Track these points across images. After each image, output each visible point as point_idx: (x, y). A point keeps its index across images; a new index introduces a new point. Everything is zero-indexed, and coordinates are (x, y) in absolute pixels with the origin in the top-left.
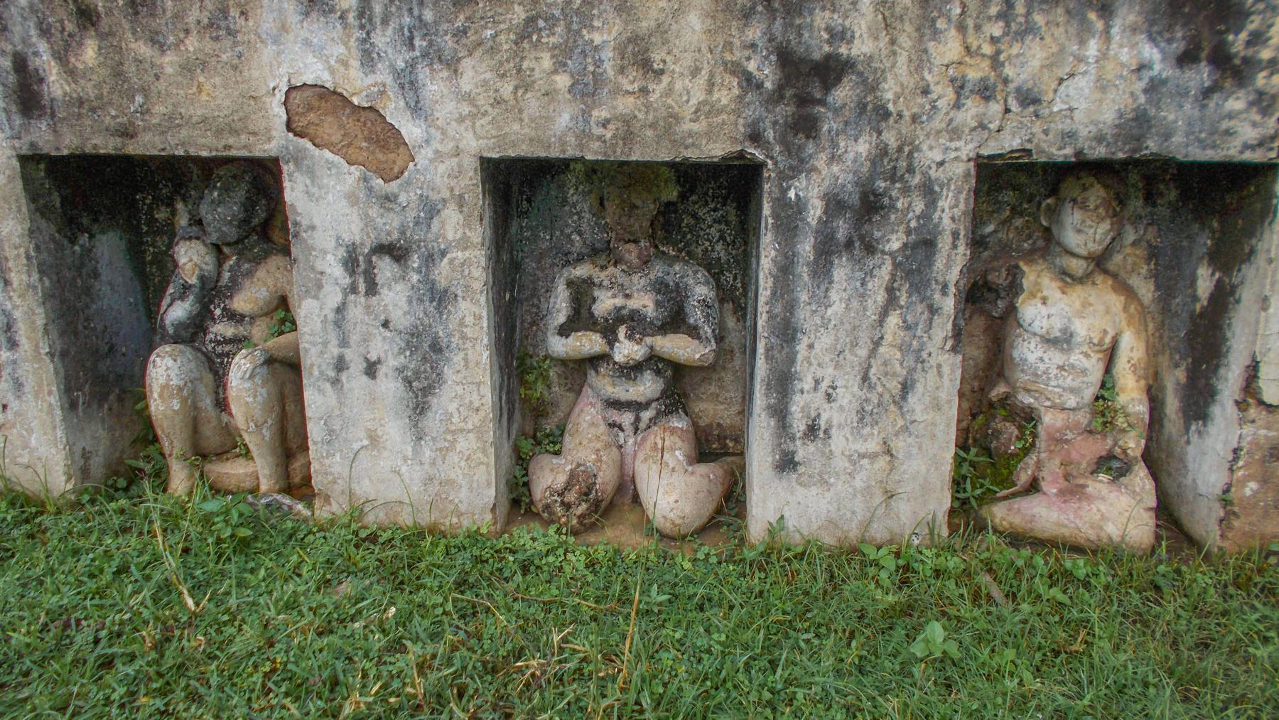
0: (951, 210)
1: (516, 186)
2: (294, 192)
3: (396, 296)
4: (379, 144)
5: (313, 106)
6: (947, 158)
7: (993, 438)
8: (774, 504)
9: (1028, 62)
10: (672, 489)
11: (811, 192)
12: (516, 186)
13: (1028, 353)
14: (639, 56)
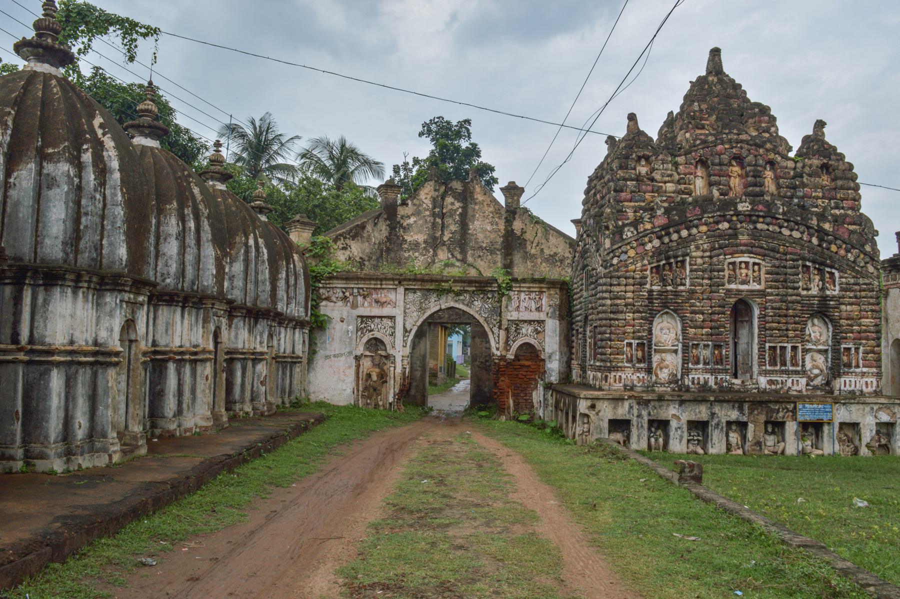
0: (724, 425)
1: (690, 423)
2: (671, 423)
3: (679, 432)
4: (679, 419)
5: (674, 415)
6: (724, 421)
7: (729, 447)
8: (712, 451)
9: (729, 414)
10: (701, 451)
11: (713, 423)
12: (690, 423)
13: (730, 439)
14: (700, 412)
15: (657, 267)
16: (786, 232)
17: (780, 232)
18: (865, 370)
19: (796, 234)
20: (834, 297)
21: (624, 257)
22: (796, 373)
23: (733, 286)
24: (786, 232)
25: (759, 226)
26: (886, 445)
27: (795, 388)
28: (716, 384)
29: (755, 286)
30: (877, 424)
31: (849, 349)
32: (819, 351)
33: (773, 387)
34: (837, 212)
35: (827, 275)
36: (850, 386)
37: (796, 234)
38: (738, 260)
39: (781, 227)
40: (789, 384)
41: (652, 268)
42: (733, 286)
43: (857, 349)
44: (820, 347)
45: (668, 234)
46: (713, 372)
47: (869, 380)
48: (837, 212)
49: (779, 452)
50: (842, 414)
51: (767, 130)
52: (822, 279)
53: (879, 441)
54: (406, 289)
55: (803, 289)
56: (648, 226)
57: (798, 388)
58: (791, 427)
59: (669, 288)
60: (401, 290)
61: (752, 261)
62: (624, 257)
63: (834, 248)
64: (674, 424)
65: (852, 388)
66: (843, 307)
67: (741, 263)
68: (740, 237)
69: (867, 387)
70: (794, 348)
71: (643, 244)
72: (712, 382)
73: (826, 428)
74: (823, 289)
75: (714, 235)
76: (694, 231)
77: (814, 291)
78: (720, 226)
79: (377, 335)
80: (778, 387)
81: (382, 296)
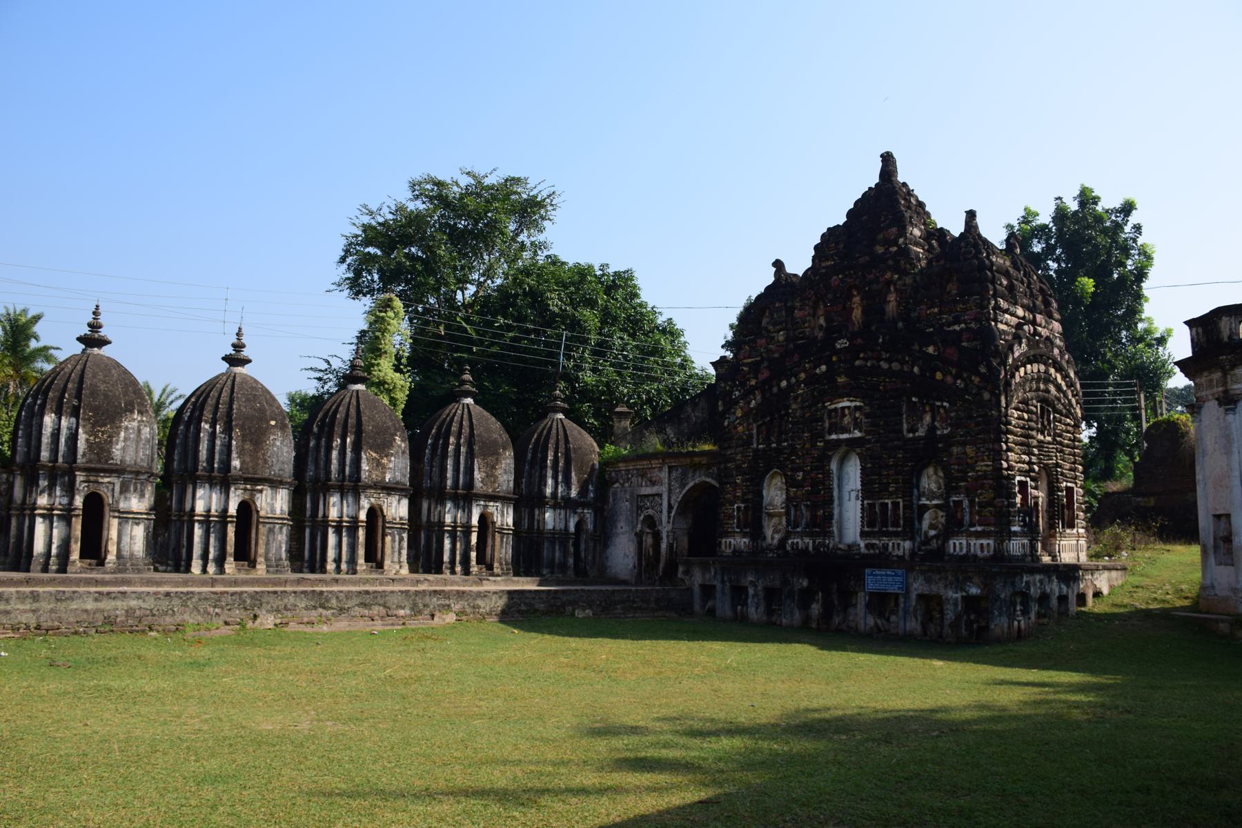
12: (766, 589)
15: (764, 423)
16: (884, 365)
17: (879, 366)
18: (979, 529)
19: (896, 366)
20: (943, 436)
21: (732, 418)
22: (896, 534)
23: (834, 437)
24: (884, 365)
25: (857, 363)
27: (896, 552)
28: (814, 548)
29: (857, 434)
31: (961, 502)
32: (937, 506)
34: (957, 328)
35: (942, 411)
36: (961, 549)
37: (896, 366)
38: (840, 405)
39: (880, 359)
41: (759, 427)
42: (834, 437)
43: (972, 503)
44: (935, 502)
45: (771, 387)
46: (812, 535)
47: (985, 542)
48: (957, 328)
51: (895, 243)
52: (933, 419)
54: (670, 468)
55: (909, 431)
56: (753, 382)
57: (900, 553)
59: (774, 445)
60: (666, 469)
61: (853, 404)
62: (732, 418)
63: (939, 376)
64: (751, 591)
66: (955, 450)
67: (843, 408)
68: (839, 380)
69: (982, 551)
70: (896, 505)
71: (749, 403)
72: (811, 548)
73: (902, 600)
74: (932, 429)
75: (812, 380)
76: (793, 380)
77: (921, 433)
78: (818, 371)
79: (650, 512)
81: (656, 474)
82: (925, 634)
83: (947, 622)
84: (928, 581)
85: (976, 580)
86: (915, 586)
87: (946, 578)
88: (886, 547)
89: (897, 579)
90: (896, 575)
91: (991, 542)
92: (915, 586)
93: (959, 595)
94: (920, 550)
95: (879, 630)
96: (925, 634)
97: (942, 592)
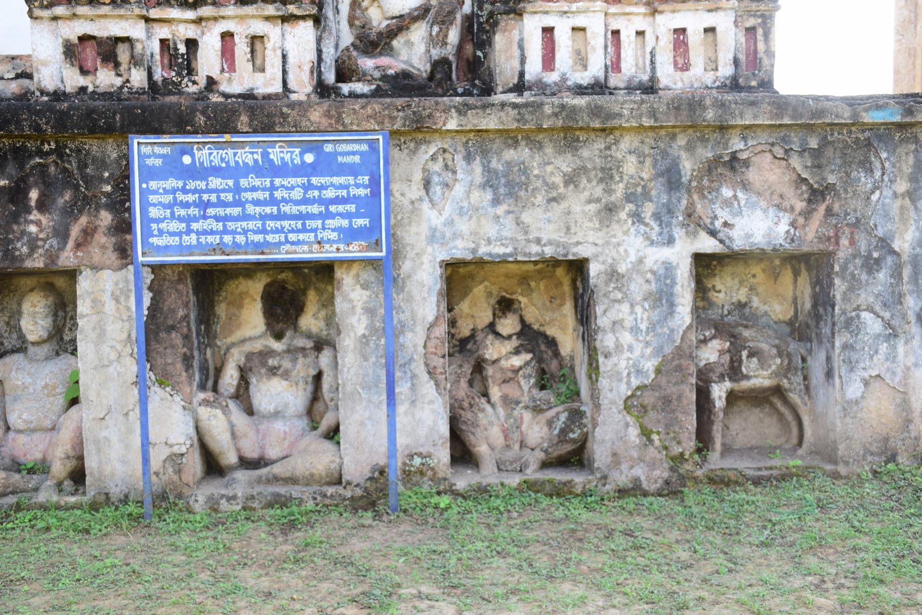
26: (778, 391)
30: (704, 264)
33: (106, 79)
40: (208, 61)
49: (60, 468)
50: (450, 212)
53: (734, 371)
58: (109, 303)
65: (596, 68)
80: (138, 78)
82: (462, 454)
83: (615, 388)
84: (508, 188)
85: (766, 172)
86: (431, 217)
87: (607, 175)
88: (182, 58)
89: (332, 185)
90: (327, 165)
91: (724, 22)
92: (431, 217)
93: (680, 253)
94: (343, 75)
95: (213, 466)
96: (462, 454)
97: (586, 242)
